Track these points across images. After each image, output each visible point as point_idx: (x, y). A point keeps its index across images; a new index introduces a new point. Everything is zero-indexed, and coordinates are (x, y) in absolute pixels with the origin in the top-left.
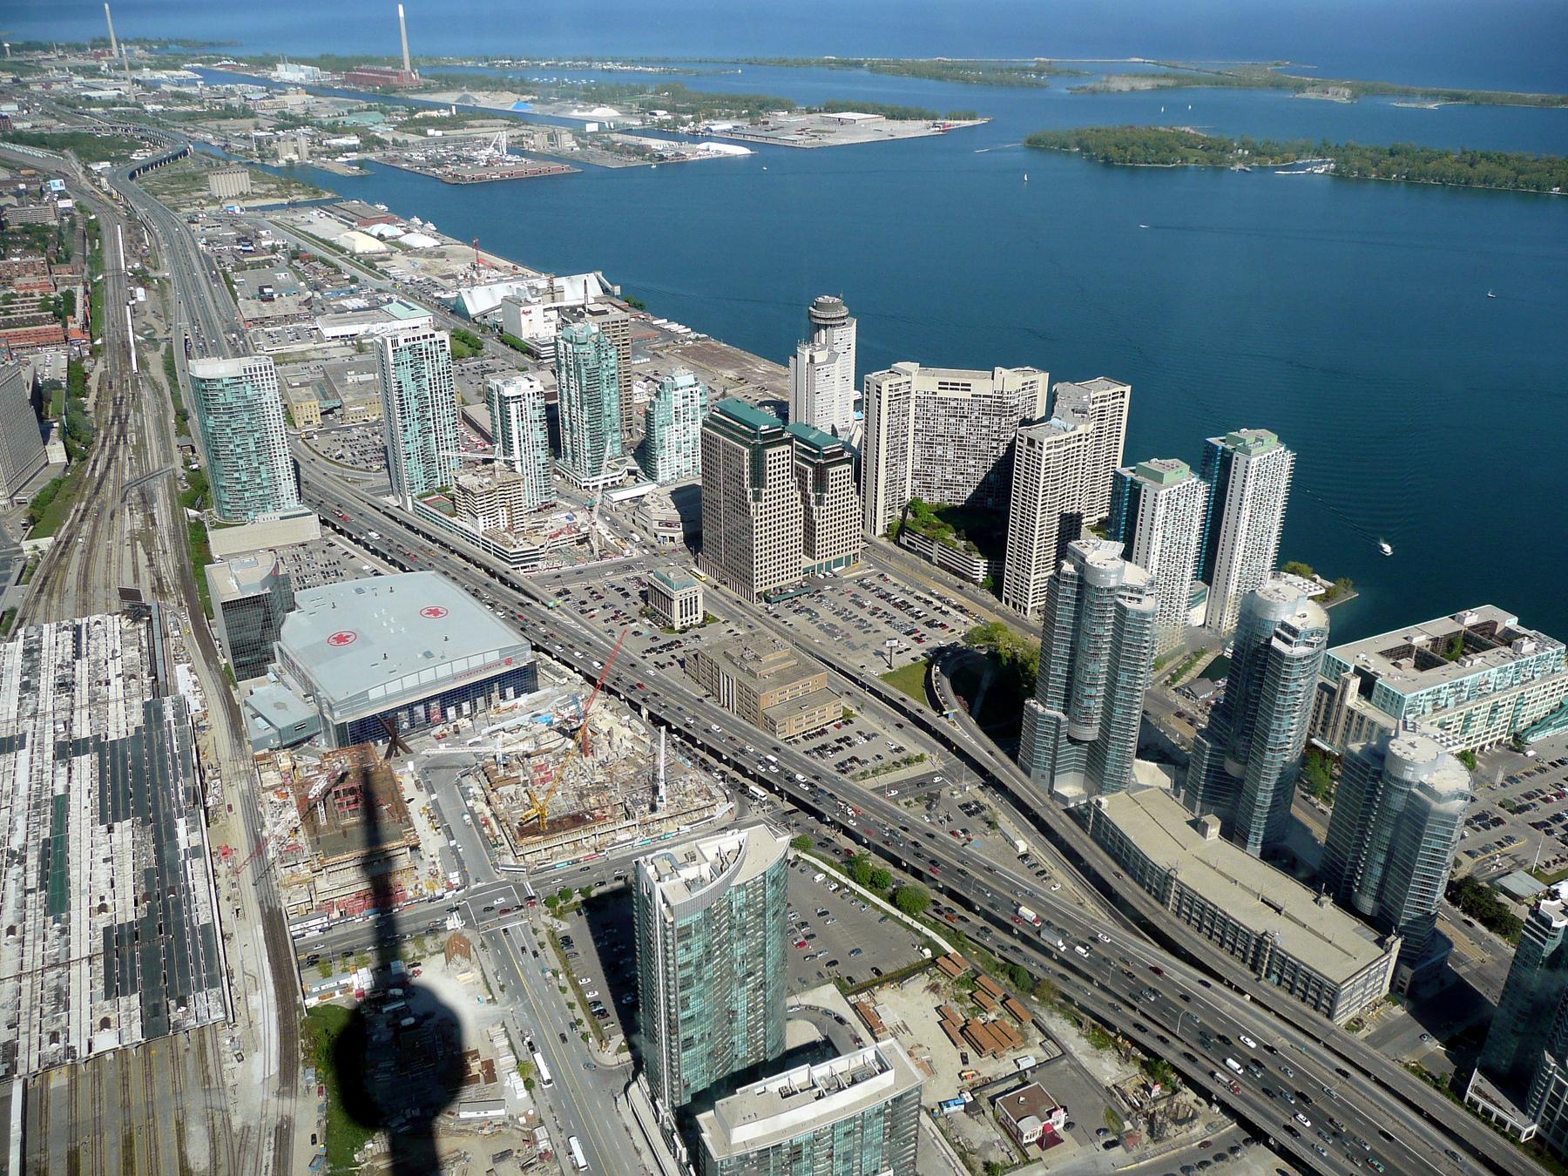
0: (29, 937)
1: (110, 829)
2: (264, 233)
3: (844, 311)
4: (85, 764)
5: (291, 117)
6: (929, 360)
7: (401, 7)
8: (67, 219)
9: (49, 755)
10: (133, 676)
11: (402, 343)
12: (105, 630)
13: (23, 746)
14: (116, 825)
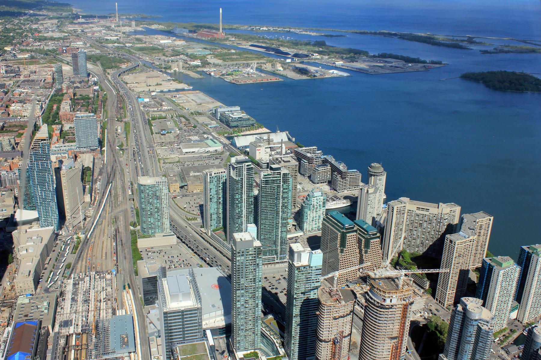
2: (164, 103)
3: (382, 169)
5: (177, 51)
6: (414, 197)
7: (221, 9)
8: (96, 93)
10: (109, 300)
11: (213, 175)
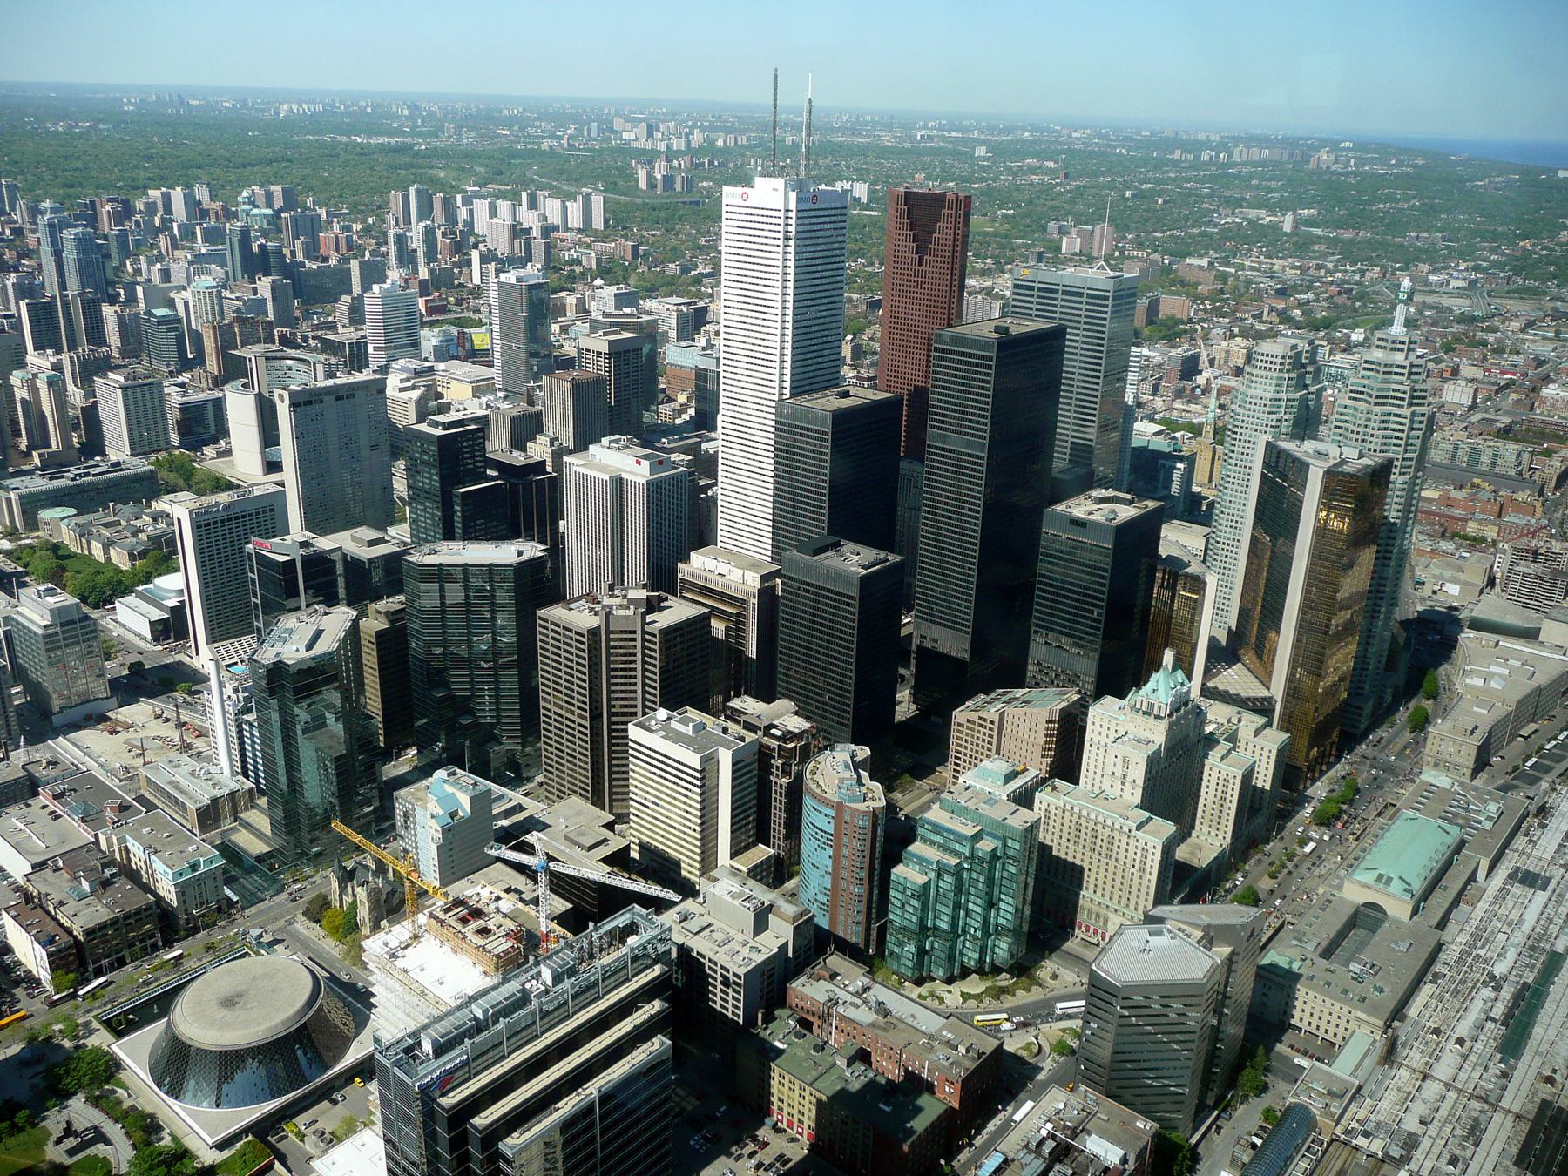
0: (1473, 1058)
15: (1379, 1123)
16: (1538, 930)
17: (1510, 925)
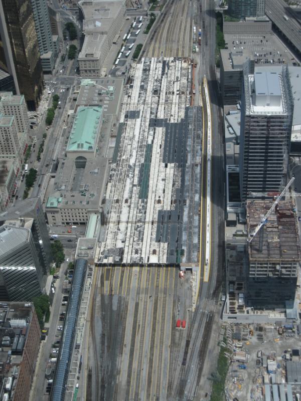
0: (132, 206)
1: (166, 166)
4: (160, 131)
9: (147, 124)
10: (183, 93)
12: (175, 66)
13: (138, 117)
14: (169, 164)
15: (108, 250)
16: (141, 137)
17: (130, 140)
